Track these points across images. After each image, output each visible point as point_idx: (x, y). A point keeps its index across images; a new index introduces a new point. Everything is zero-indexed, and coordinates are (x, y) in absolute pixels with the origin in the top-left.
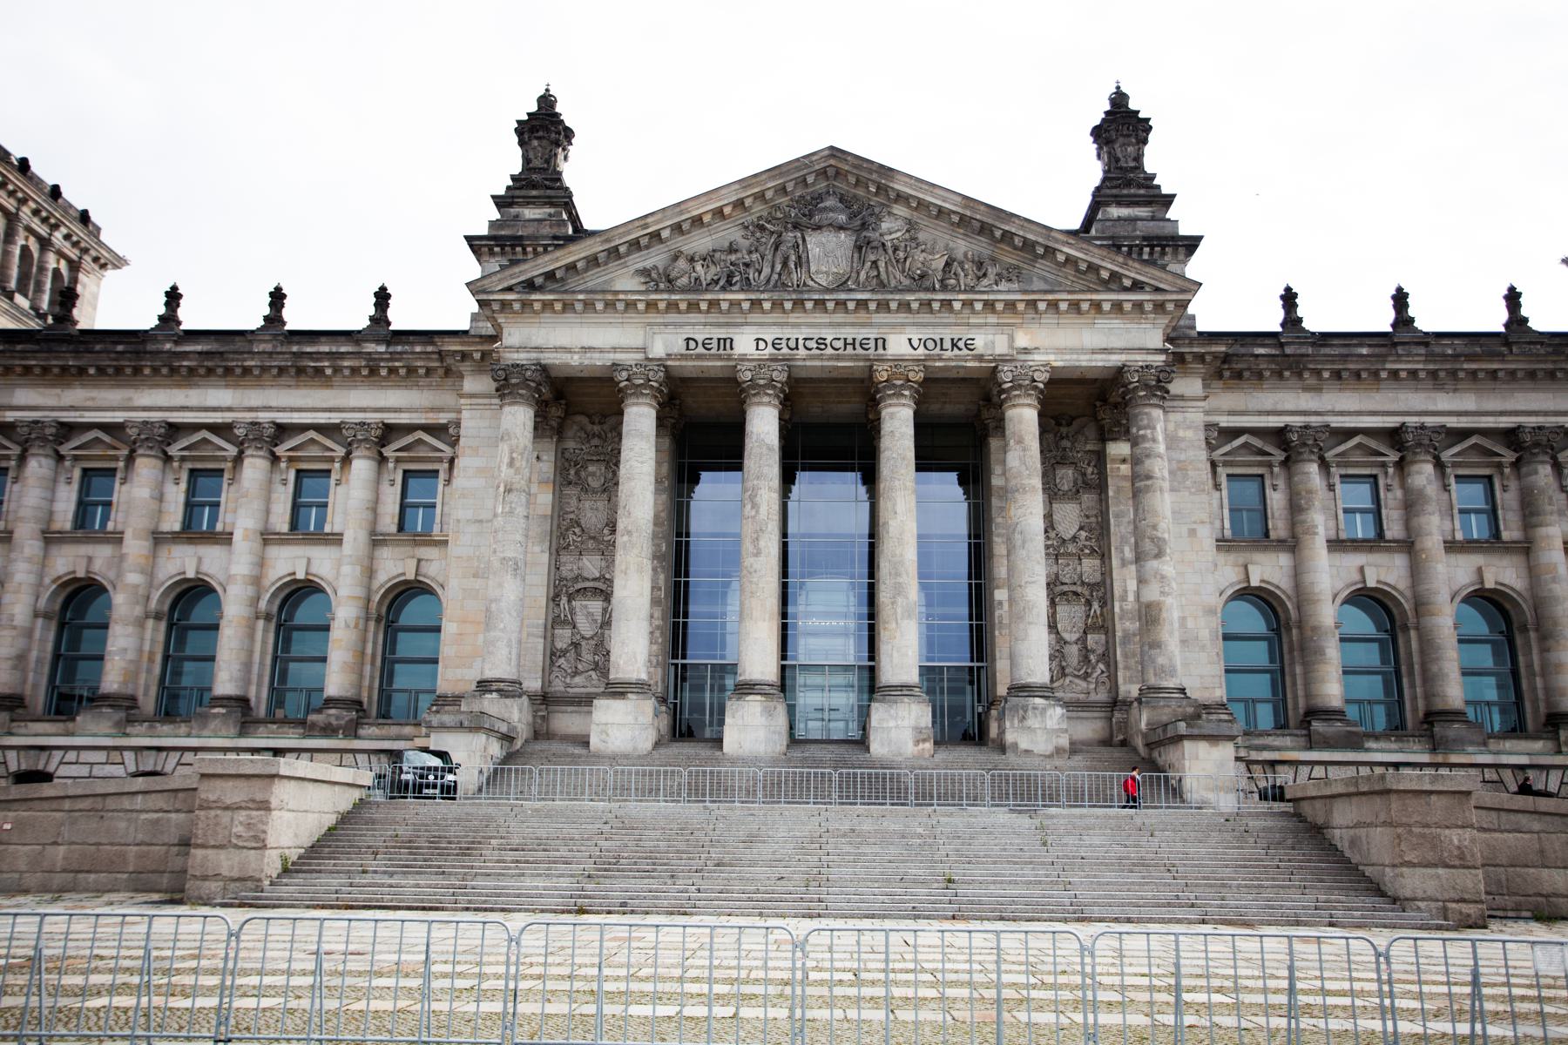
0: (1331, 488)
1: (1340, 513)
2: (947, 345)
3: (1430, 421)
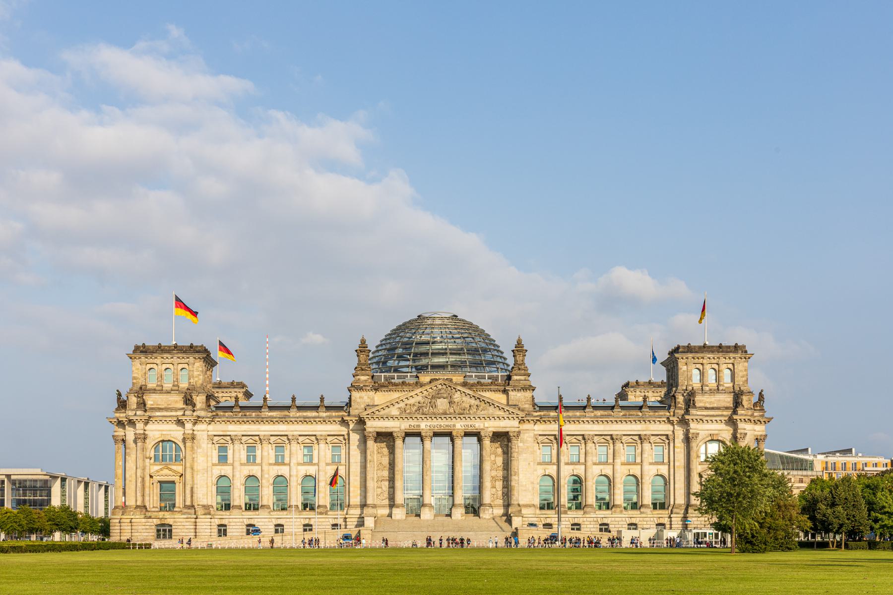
0: (567, 449)
1: (569, 455)
2: (470, 426)
3: (591, 433)
